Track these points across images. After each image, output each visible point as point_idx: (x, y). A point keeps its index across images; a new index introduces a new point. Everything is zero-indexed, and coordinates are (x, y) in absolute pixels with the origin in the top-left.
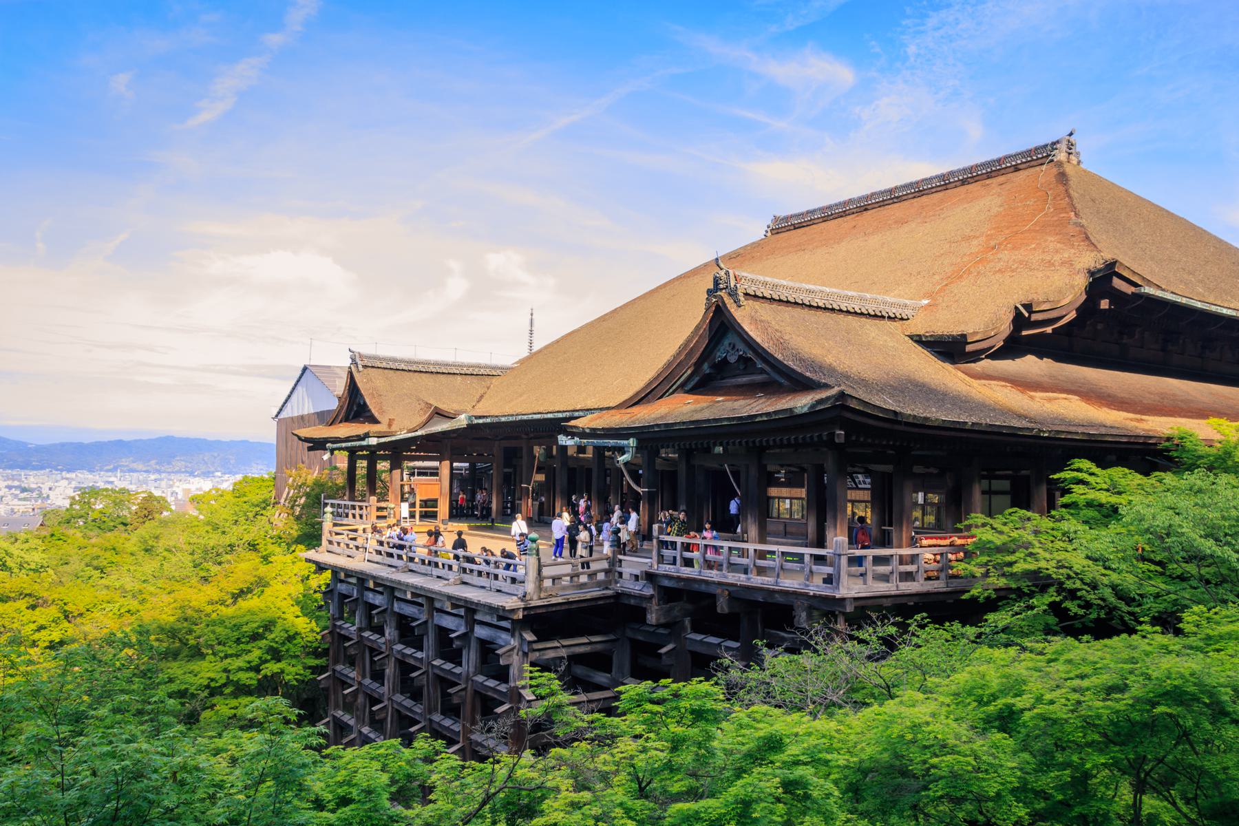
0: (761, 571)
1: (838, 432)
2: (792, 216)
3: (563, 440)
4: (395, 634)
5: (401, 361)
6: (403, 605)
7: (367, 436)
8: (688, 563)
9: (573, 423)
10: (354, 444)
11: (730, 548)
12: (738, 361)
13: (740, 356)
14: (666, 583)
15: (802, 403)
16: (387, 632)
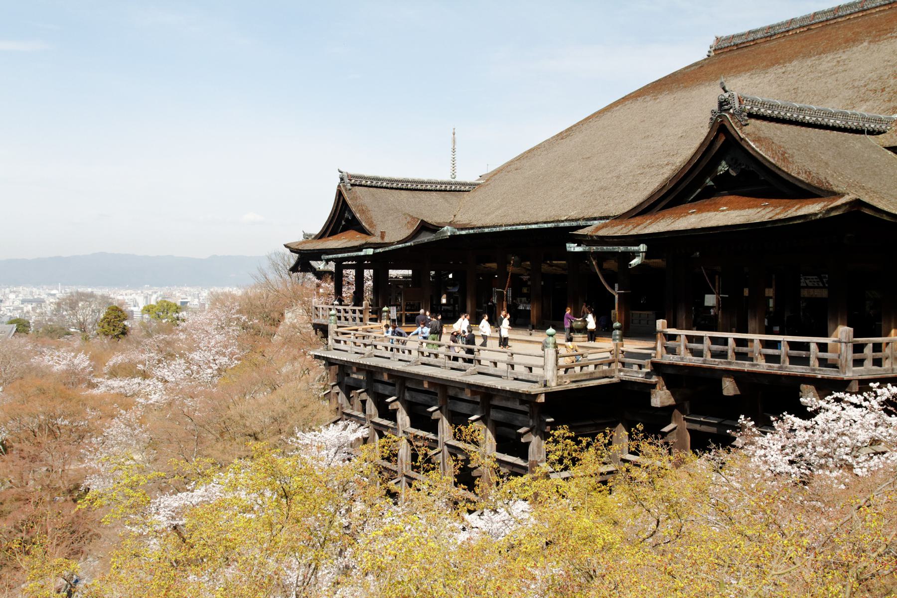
2: (733, 37)
3: (573, 247)
5: (383, 180)
6: (414, 393)
7: (360, 248)
9: (580, 232)
10: (340, 256)
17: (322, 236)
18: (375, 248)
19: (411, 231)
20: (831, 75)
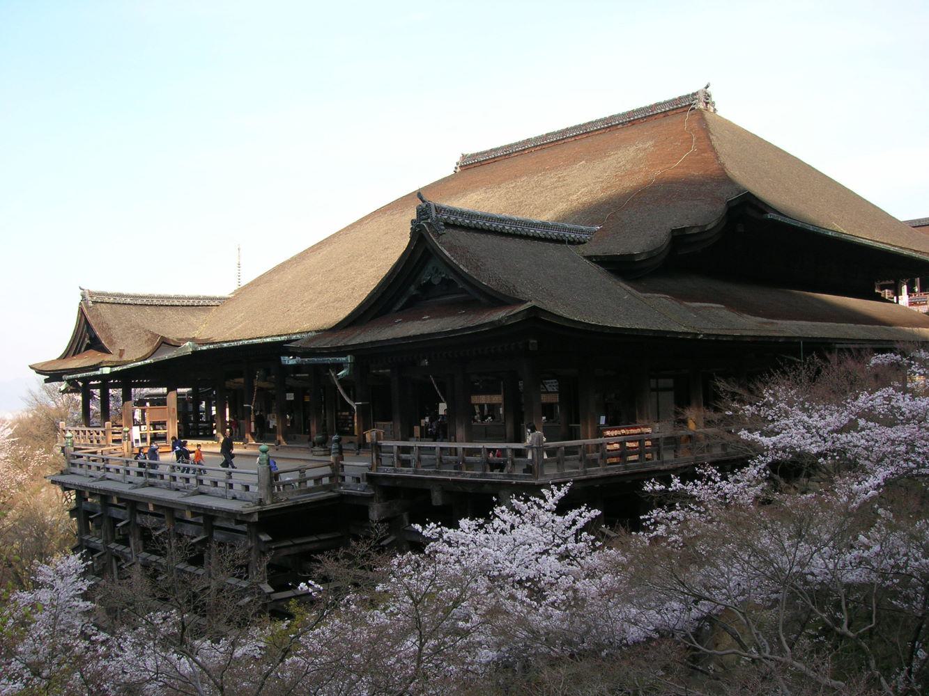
0: (470, 466)
1: (532, 341)
2: (477, 154)
3: (289, 361)
4: (140, 543)
5: (127, 296)
7: (96, 367)
8: (406, 463)
11: (442, 449)
12: (441, 283)
13: (443, 278)
14: (385, 483)
15: (499, 315)
16: (132, 542)
17: (66, 356)
18: (111, 367)
19: (151, 348)
20: (551, 189)
